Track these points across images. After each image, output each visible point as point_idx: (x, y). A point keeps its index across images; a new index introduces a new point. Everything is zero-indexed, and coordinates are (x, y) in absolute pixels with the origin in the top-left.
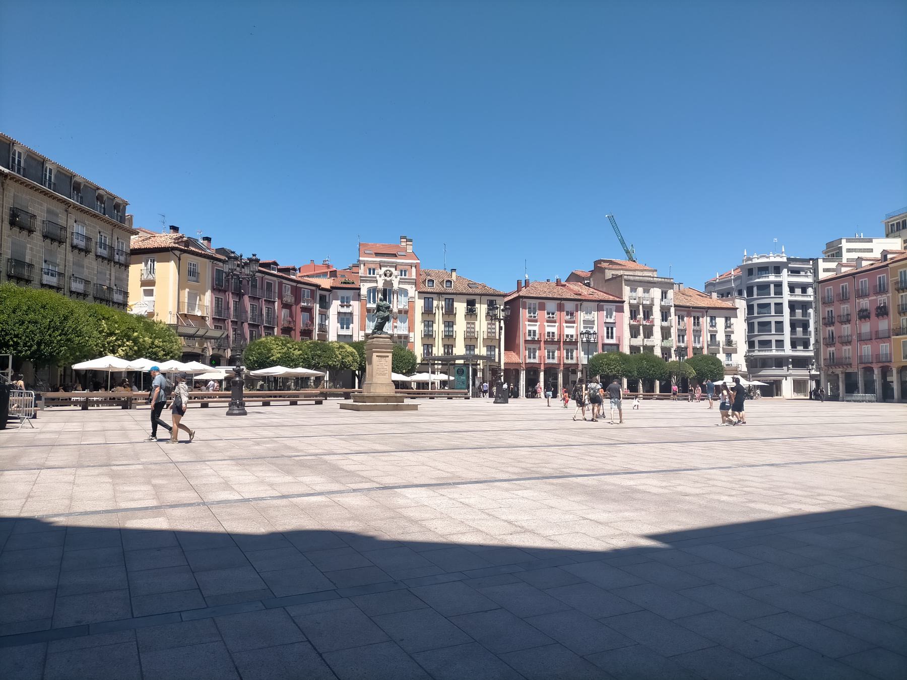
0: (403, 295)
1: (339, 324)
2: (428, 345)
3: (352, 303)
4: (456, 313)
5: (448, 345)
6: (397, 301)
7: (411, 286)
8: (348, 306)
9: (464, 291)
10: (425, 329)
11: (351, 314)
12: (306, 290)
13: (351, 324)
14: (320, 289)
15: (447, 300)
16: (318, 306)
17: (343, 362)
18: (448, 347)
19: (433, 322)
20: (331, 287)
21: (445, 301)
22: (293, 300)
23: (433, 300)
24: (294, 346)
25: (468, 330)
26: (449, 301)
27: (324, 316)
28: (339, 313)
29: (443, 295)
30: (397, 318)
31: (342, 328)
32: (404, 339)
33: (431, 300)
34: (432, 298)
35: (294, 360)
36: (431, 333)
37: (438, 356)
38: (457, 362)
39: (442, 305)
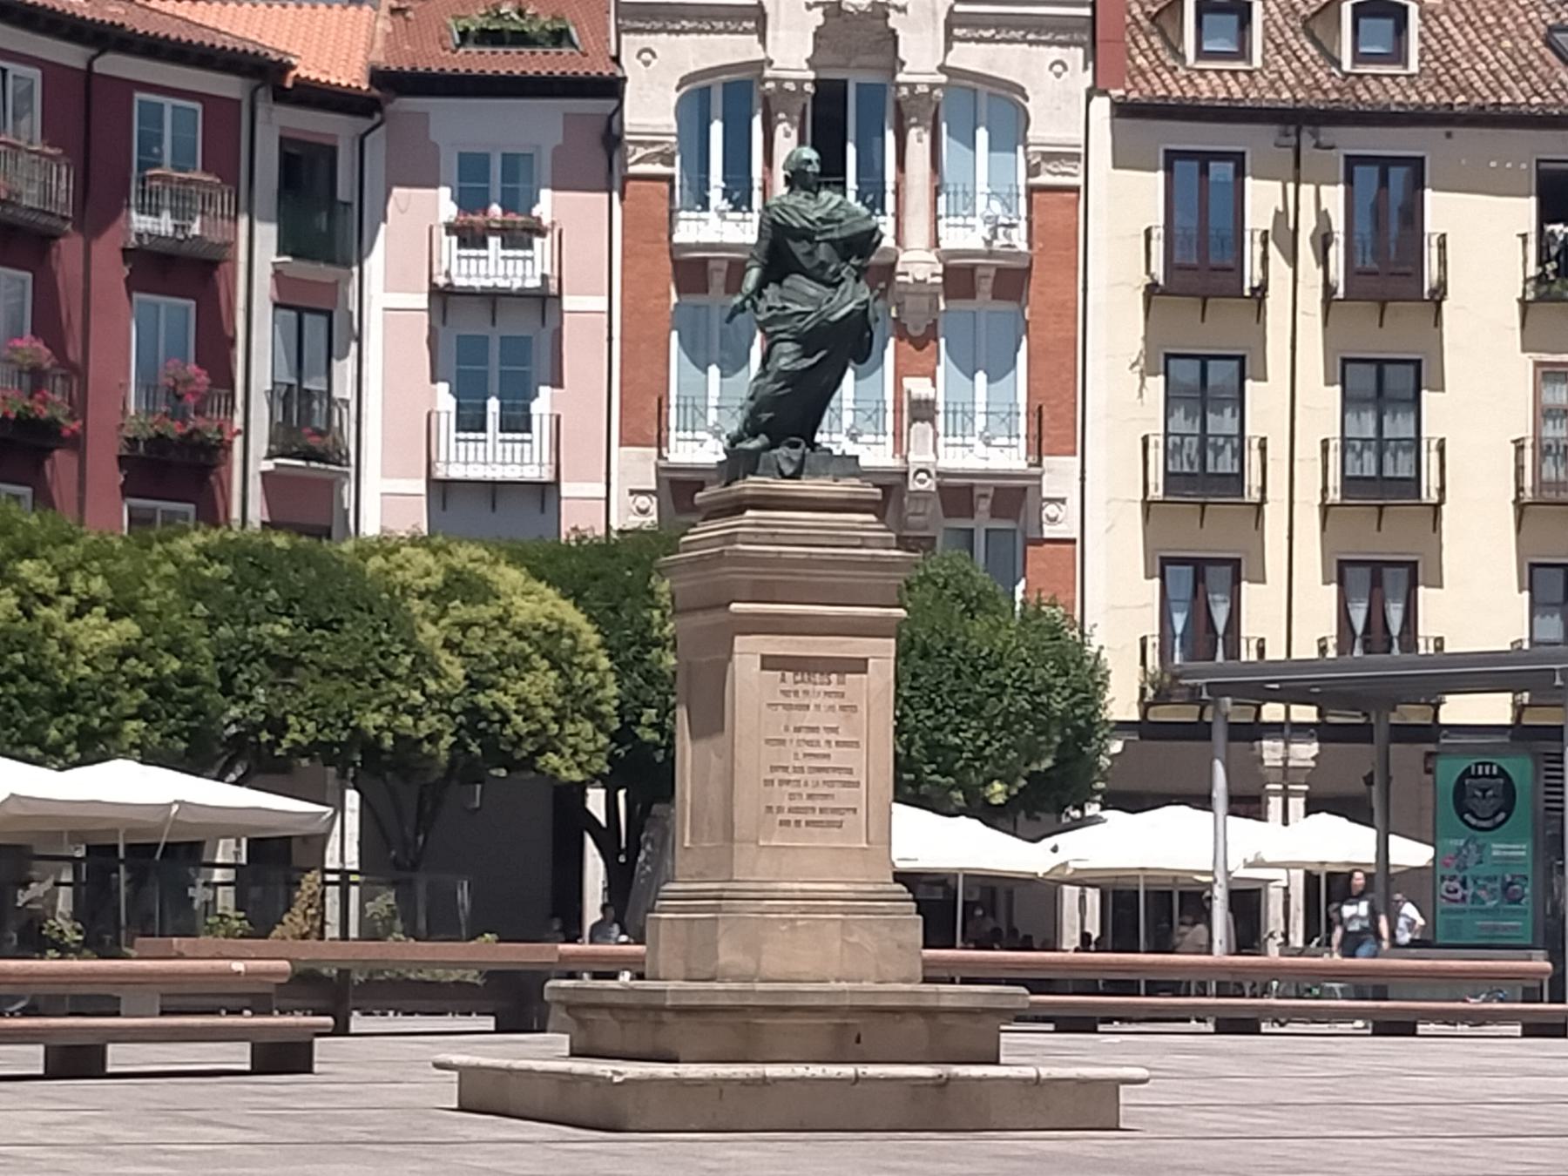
0: (982, 135)
1: (443, 387)
2: (1199, 566)
3: (547, 205)
4: (1440, 291)
5: (1377, 569)
6: (937, 192)
7: (1056, 53)
8: (520, 236)
9: (1516, 96)
10: (1180, 423)
11: (544, 301)
12: (169, 102)
13: (545, 391)
14: (282, 96)
15: (1367, 176)
16: (267, 234)
17: (474, 712)
18: (1376, 582)
19: (1246, 365)
20: (378, 77)
21: (1349, 181)
22: (63, 185)
23: (1240, 173)
24: (77, 582)
25: (1551, 431)
26: (1384, 181)
27: (314, 326)
28: (443, 297)
29: (1328, 134)
30: (931, 334)
31: (470, 421)
32: (994, 514)
33: (1221, 171)
34: (1238, 159)
35: (71, 694)
36: (1226, 465)
37: (1289, 664)
38: (1458, 709)
39: (1323, 217)
